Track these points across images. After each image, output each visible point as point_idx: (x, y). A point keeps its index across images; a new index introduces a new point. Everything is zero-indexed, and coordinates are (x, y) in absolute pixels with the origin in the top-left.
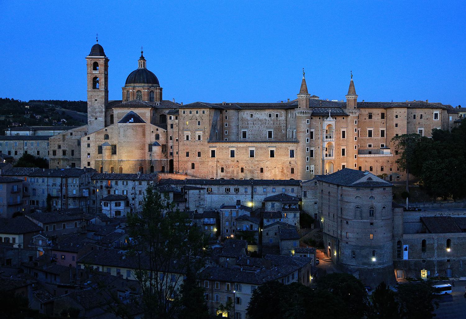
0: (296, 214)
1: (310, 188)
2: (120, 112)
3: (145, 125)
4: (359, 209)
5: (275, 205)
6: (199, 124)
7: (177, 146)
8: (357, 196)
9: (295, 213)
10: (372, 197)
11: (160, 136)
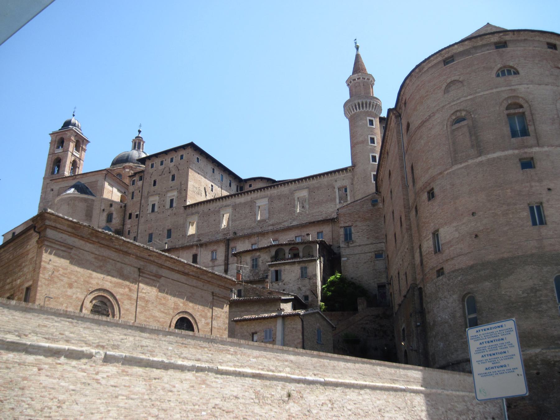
0: (306, 268)
1: (359, 217)
2: (62, 186)
3: (93, 201)
4: (463, 123)
5: (260, 261)
6: (173, 179)
7: (136, 227)
8: (449, 81)
9: (303, 265)
10: (508, 71)
11: (115, 216)
